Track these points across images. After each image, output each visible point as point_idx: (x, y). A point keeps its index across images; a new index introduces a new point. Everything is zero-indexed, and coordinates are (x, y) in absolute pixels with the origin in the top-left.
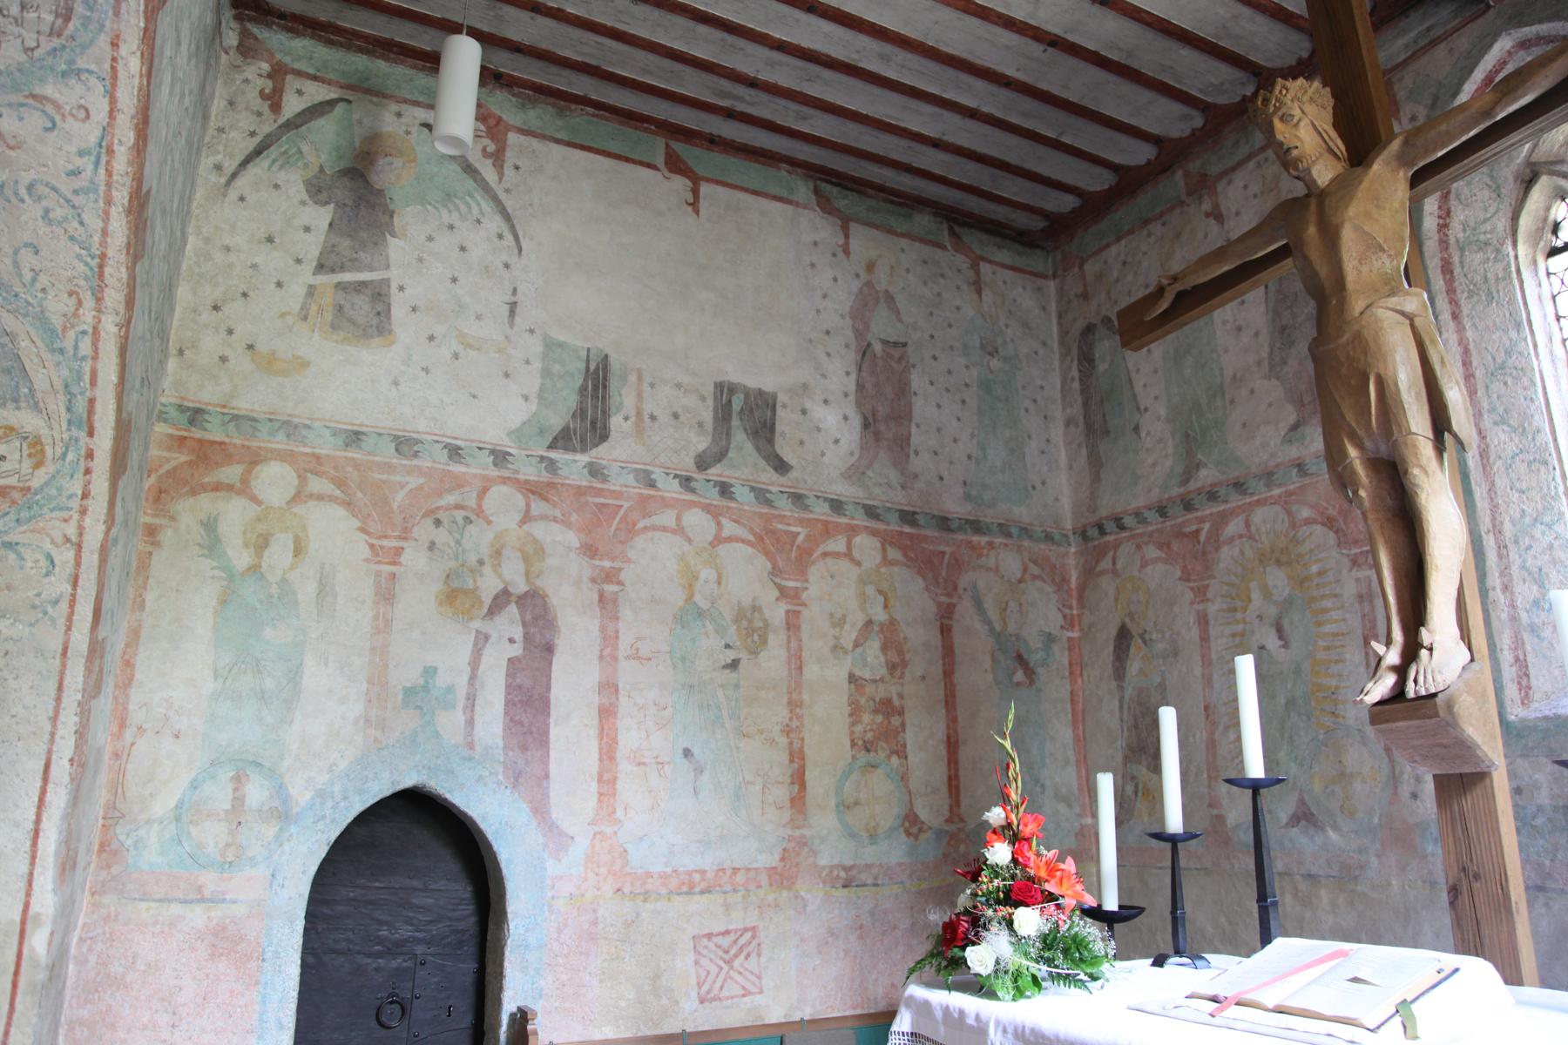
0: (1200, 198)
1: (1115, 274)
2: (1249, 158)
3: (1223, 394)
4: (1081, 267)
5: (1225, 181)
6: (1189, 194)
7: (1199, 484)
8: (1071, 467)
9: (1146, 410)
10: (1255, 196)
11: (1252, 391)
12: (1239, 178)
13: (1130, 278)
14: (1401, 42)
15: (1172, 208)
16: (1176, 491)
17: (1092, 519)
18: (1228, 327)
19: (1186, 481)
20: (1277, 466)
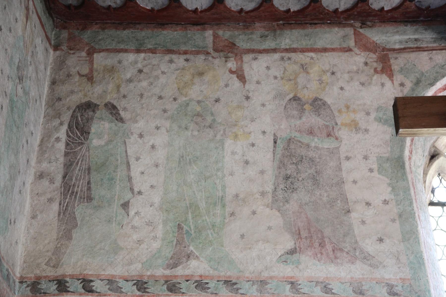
0: (227, 57)
1: (128, 76)
2: (275, 51)
3: (224, 206)
4: (90, 53)
5: (251, 56)
6: (216, 50)
7: (187, 272)
8: (34, 217)
9: (140, 193)
10: (276, 78)
11: (254, 213)
12: (264, 60)
13: (144, 84)
14: (397, 37)
15: (198, 53)
16: (160, 272)
17: (51, 273)
18: (237, 157)
19: (175, 266)
20: (271, 278)
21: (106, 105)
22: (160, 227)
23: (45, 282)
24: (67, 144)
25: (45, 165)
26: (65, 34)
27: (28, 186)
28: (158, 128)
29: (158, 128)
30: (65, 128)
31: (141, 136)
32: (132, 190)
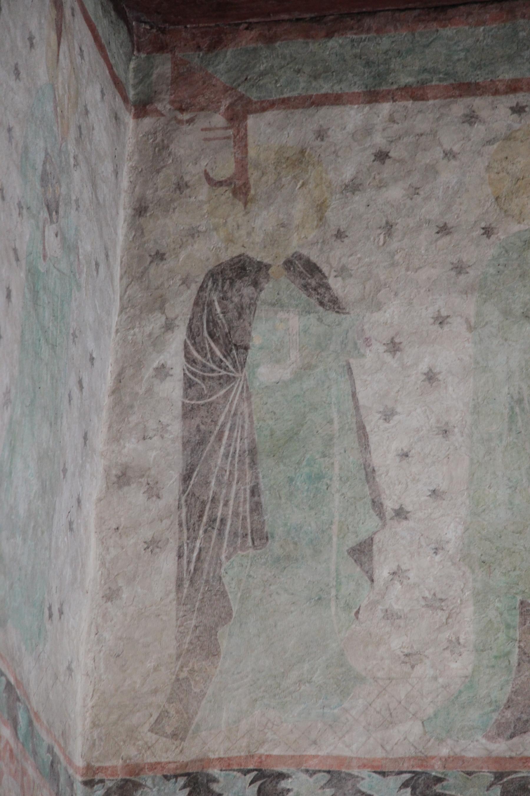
1: (348, 173)
4: (236, 117)
8: (111, 595)
9: (401, 514)
13: (395, 193)
17: (168, 754)
21: (289, 264)
22: (469, 611)
23: (153, 780)
24: (189, 384)
25: (131, 446)
26: (163, 67)
27: (90, 509)
28: (441, 321)
29: (441, 321)
30: (179, 336)
31: (394, 347)
32: (377, 505)
